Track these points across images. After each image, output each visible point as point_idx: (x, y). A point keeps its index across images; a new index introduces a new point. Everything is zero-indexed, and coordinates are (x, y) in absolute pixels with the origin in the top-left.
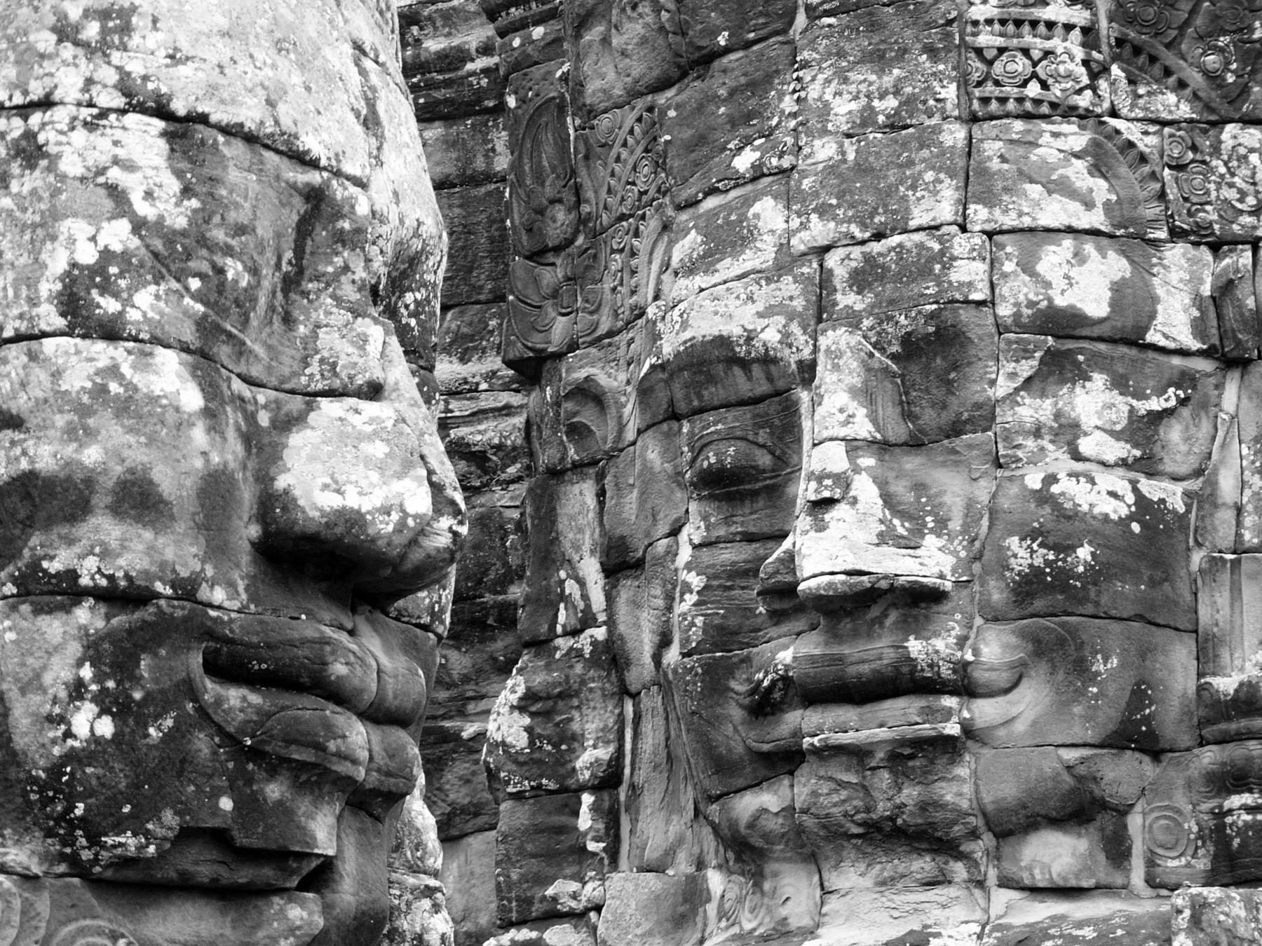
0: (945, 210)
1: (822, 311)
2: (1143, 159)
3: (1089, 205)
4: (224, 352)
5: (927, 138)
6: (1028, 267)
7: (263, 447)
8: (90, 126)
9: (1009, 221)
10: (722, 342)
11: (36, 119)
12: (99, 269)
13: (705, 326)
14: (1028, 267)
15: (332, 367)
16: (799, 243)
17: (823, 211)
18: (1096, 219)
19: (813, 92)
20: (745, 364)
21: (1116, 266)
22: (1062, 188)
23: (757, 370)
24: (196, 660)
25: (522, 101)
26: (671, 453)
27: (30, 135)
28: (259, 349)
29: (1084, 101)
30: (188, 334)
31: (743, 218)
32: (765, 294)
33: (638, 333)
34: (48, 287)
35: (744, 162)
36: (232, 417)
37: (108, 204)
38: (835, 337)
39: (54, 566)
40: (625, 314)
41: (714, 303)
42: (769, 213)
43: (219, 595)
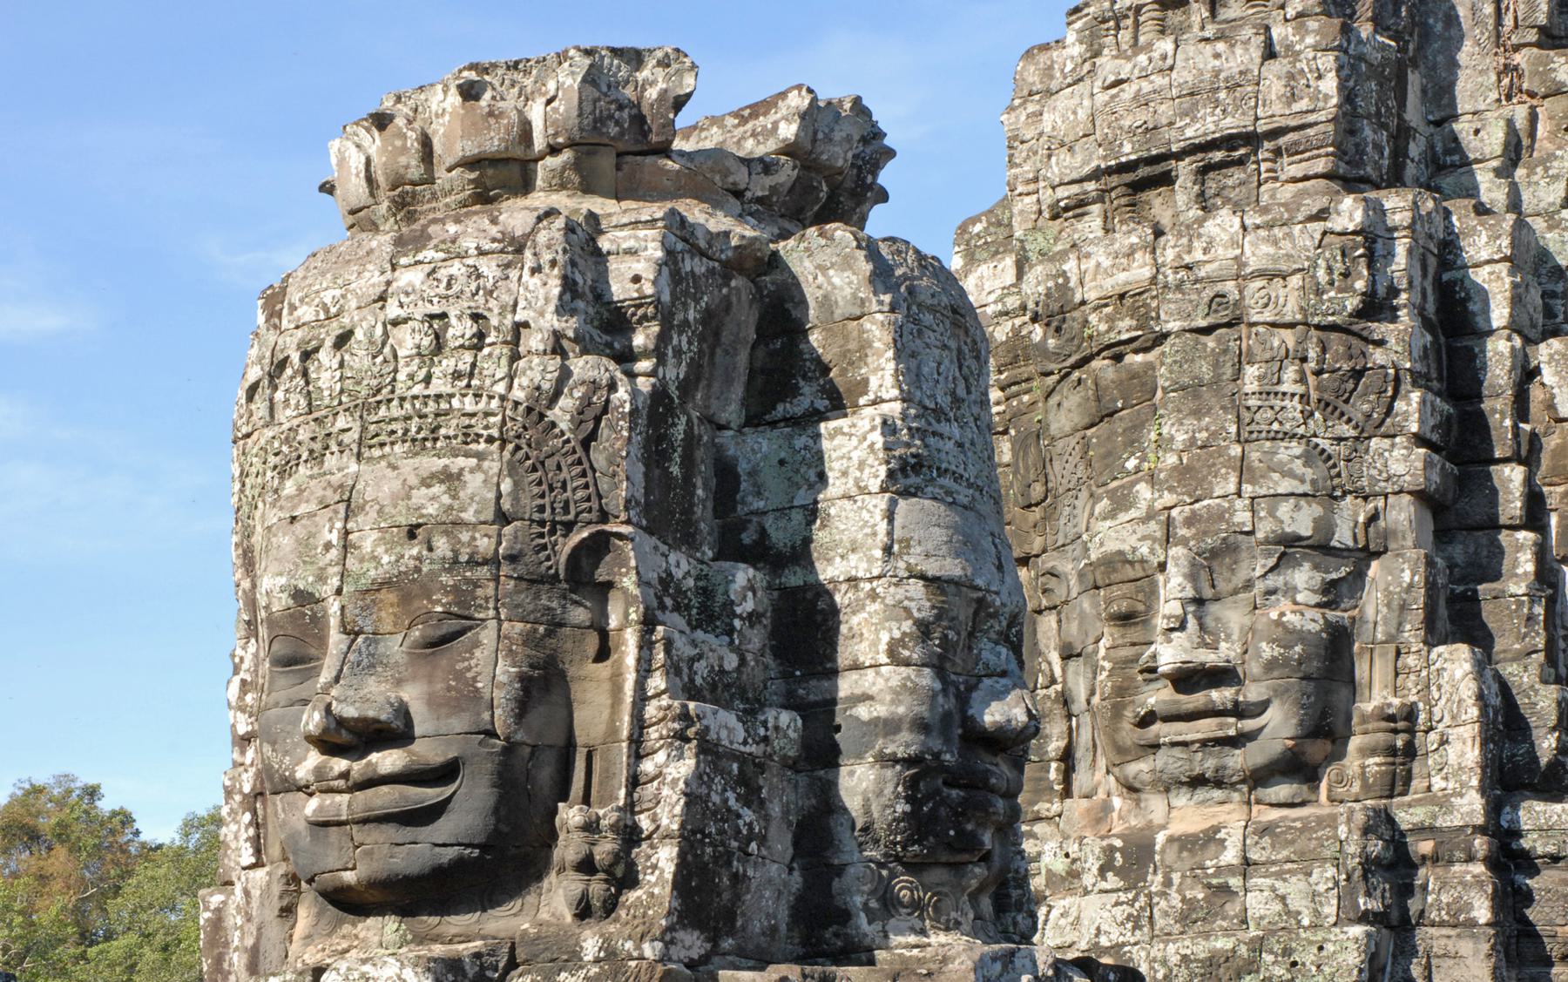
0: (1232, 488)
1: (1168, 539)
2: (1330, 457)
3: (1303, 481)
4: (948, 665)
5: (1221, 452)
6: (1272, 513)
7: (963, 700)
8: (896, 585)
9: (1263, 492)
10: (1121, 553)
11: (875, 583)
12: (902, 639)
13: (1112, 546)
14: (1272, 513)
15: (987, 665)
16: (1158, 505)
17: (1171, 489)
18: (1307, 488)
19: (1165, 431)
20: (1131, 563)
21: (1316, 510)
22: (1291, 474)
23: (1137, 566)
24: (940, 781)
25: (1018, 432)
26: (1096, 605)
27: (873, 590)
28: (958, 661)
29: (1301, 430)
30: (935, 661)
31: (1130, 492)
32: (1142, 530)
33: (1078, 545)
34: (883, 647)
35: (1131, 464)
36: (952, 690)
37: (904, 614)
38: (1177, 551)
39: (887, 751)
40: (1071, 537)
41: (1115, 535)
42: (1143, 491)
43: (948, 757)
